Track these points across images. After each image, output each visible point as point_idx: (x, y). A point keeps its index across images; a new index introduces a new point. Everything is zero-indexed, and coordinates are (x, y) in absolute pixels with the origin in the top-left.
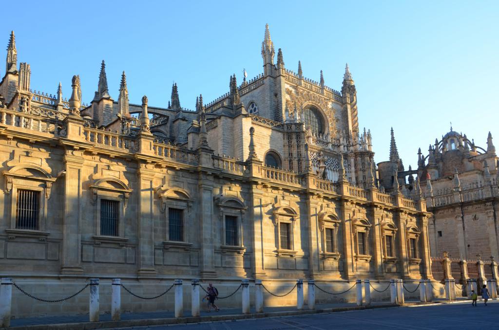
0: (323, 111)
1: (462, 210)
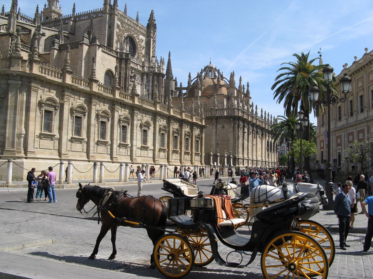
0: (136, 41)
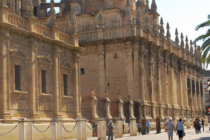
1: (104, 48)
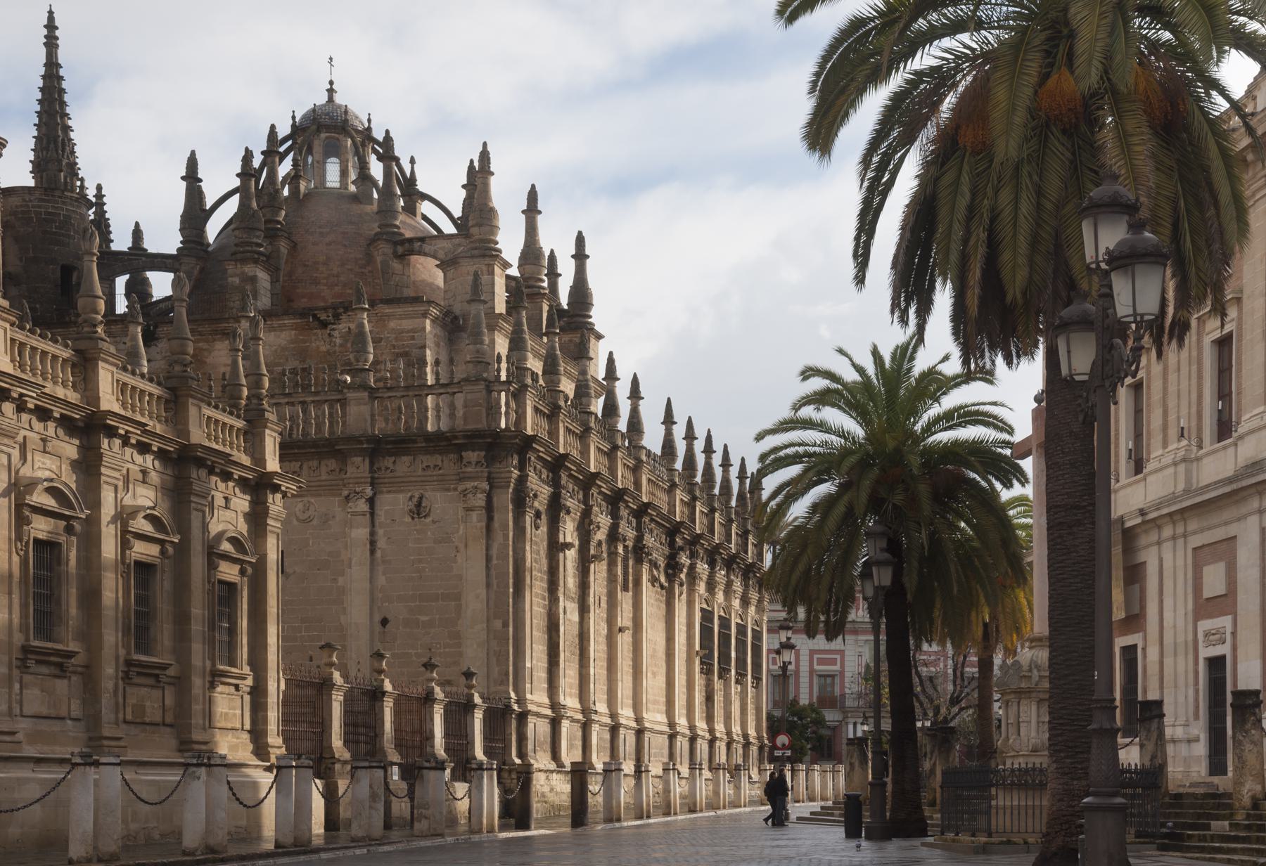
1: (372, 471)
